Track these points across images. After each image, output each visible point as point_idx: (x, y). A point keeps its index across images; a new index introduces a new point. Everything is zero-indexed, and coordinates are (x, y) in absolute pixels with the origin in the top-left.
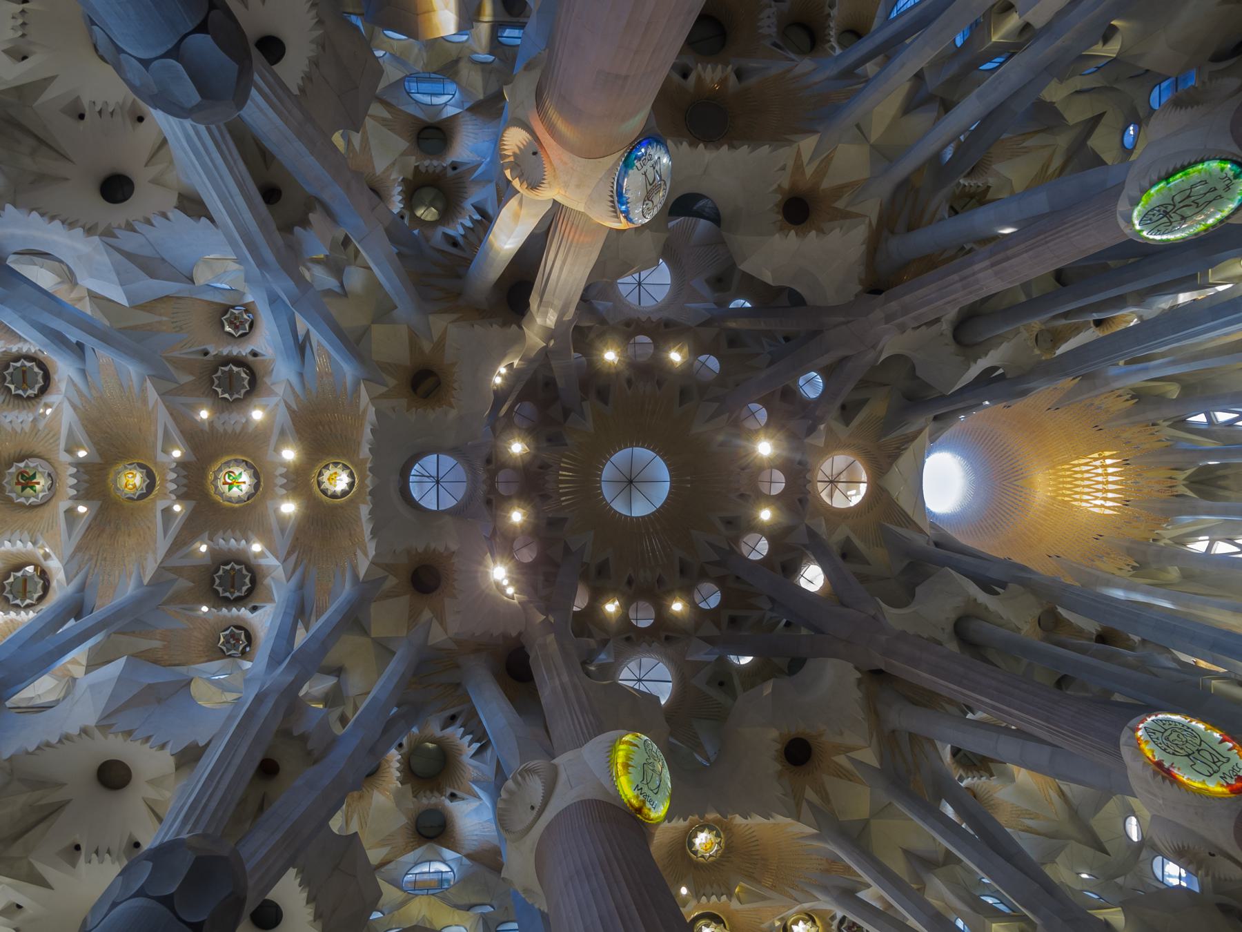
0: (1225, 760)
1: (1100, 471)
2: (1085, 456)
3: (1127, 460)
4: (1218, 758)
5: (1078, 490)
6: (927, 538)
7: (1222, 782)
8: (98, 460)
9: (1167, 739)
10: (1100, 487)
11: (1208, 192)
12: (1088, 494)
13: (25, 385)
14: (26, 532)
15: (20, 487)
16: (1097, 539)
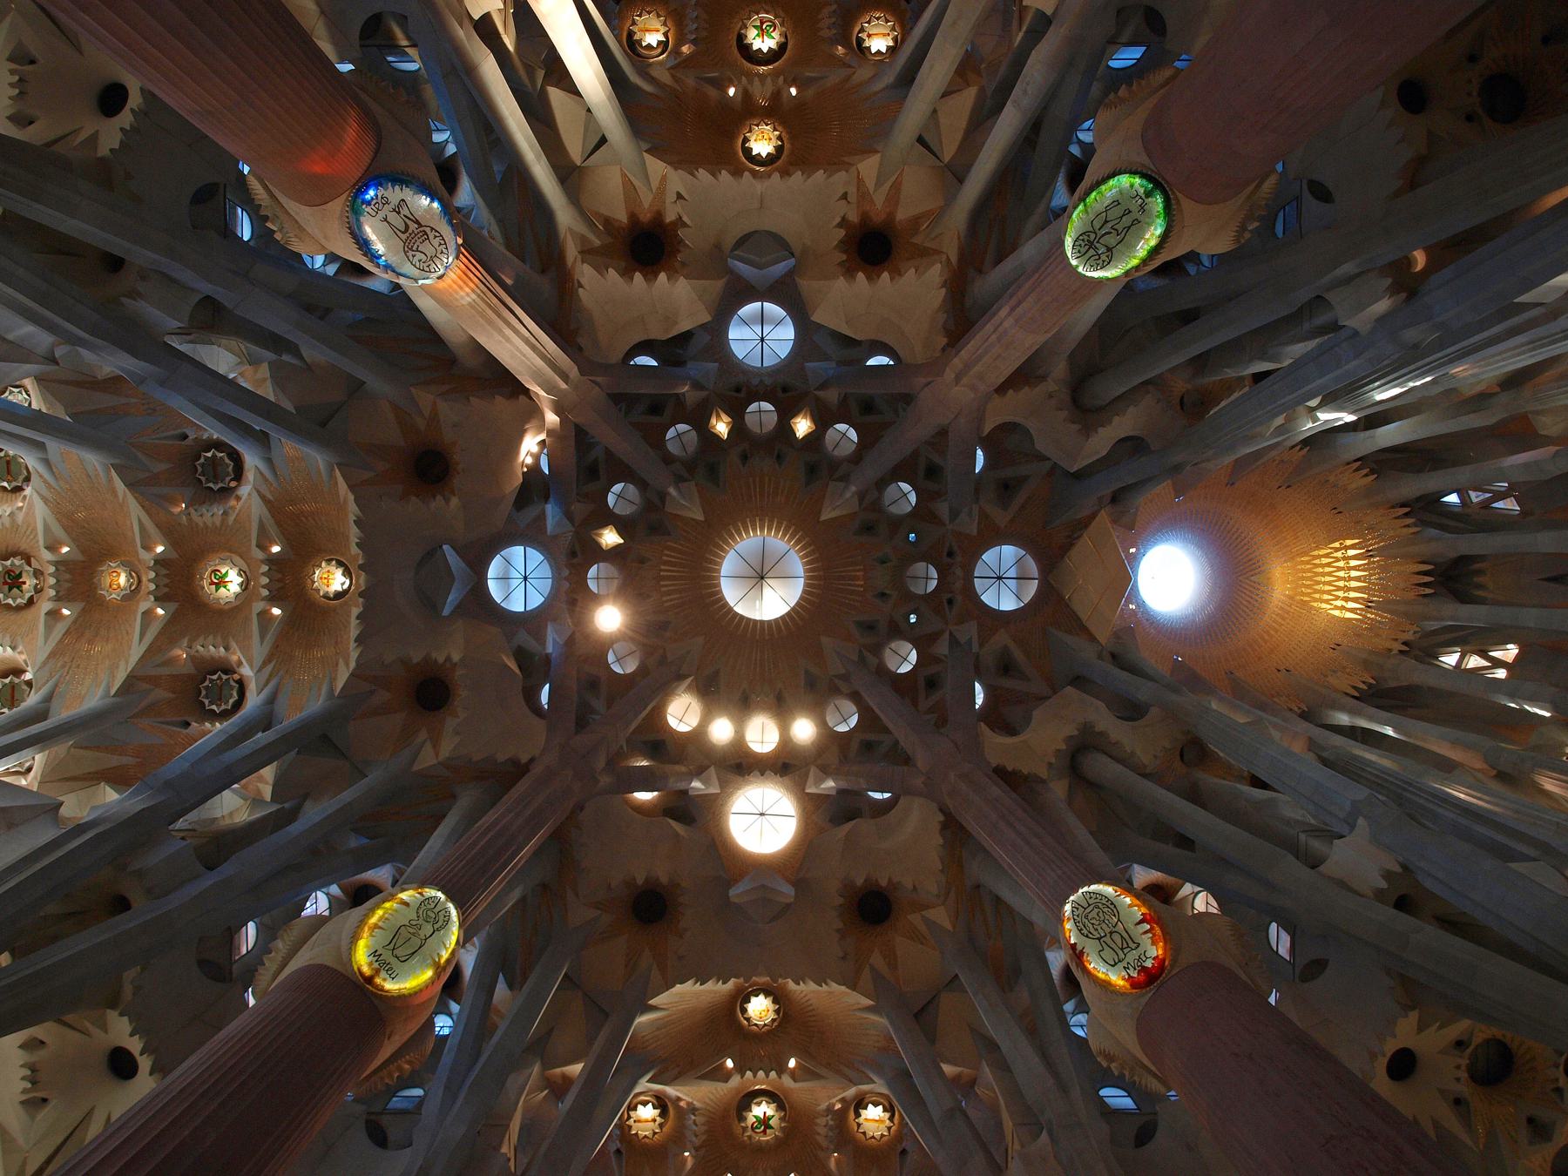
0: (1133, 946)
1: (1341, 564)
2: (1326, 546)
3: (1370, 551)
4: (1127, 944)
5: (1317, 587)
6: (1100, 647)
7: (1124, 973)
8: (80, 557)
9: (1086, 917)
10: (1341, 584)
11: (1124, 215)
12: (1328, 593)
13: (9, 477)
14: (8, 636)
15: (7, 587)
16: (1334, 649)
